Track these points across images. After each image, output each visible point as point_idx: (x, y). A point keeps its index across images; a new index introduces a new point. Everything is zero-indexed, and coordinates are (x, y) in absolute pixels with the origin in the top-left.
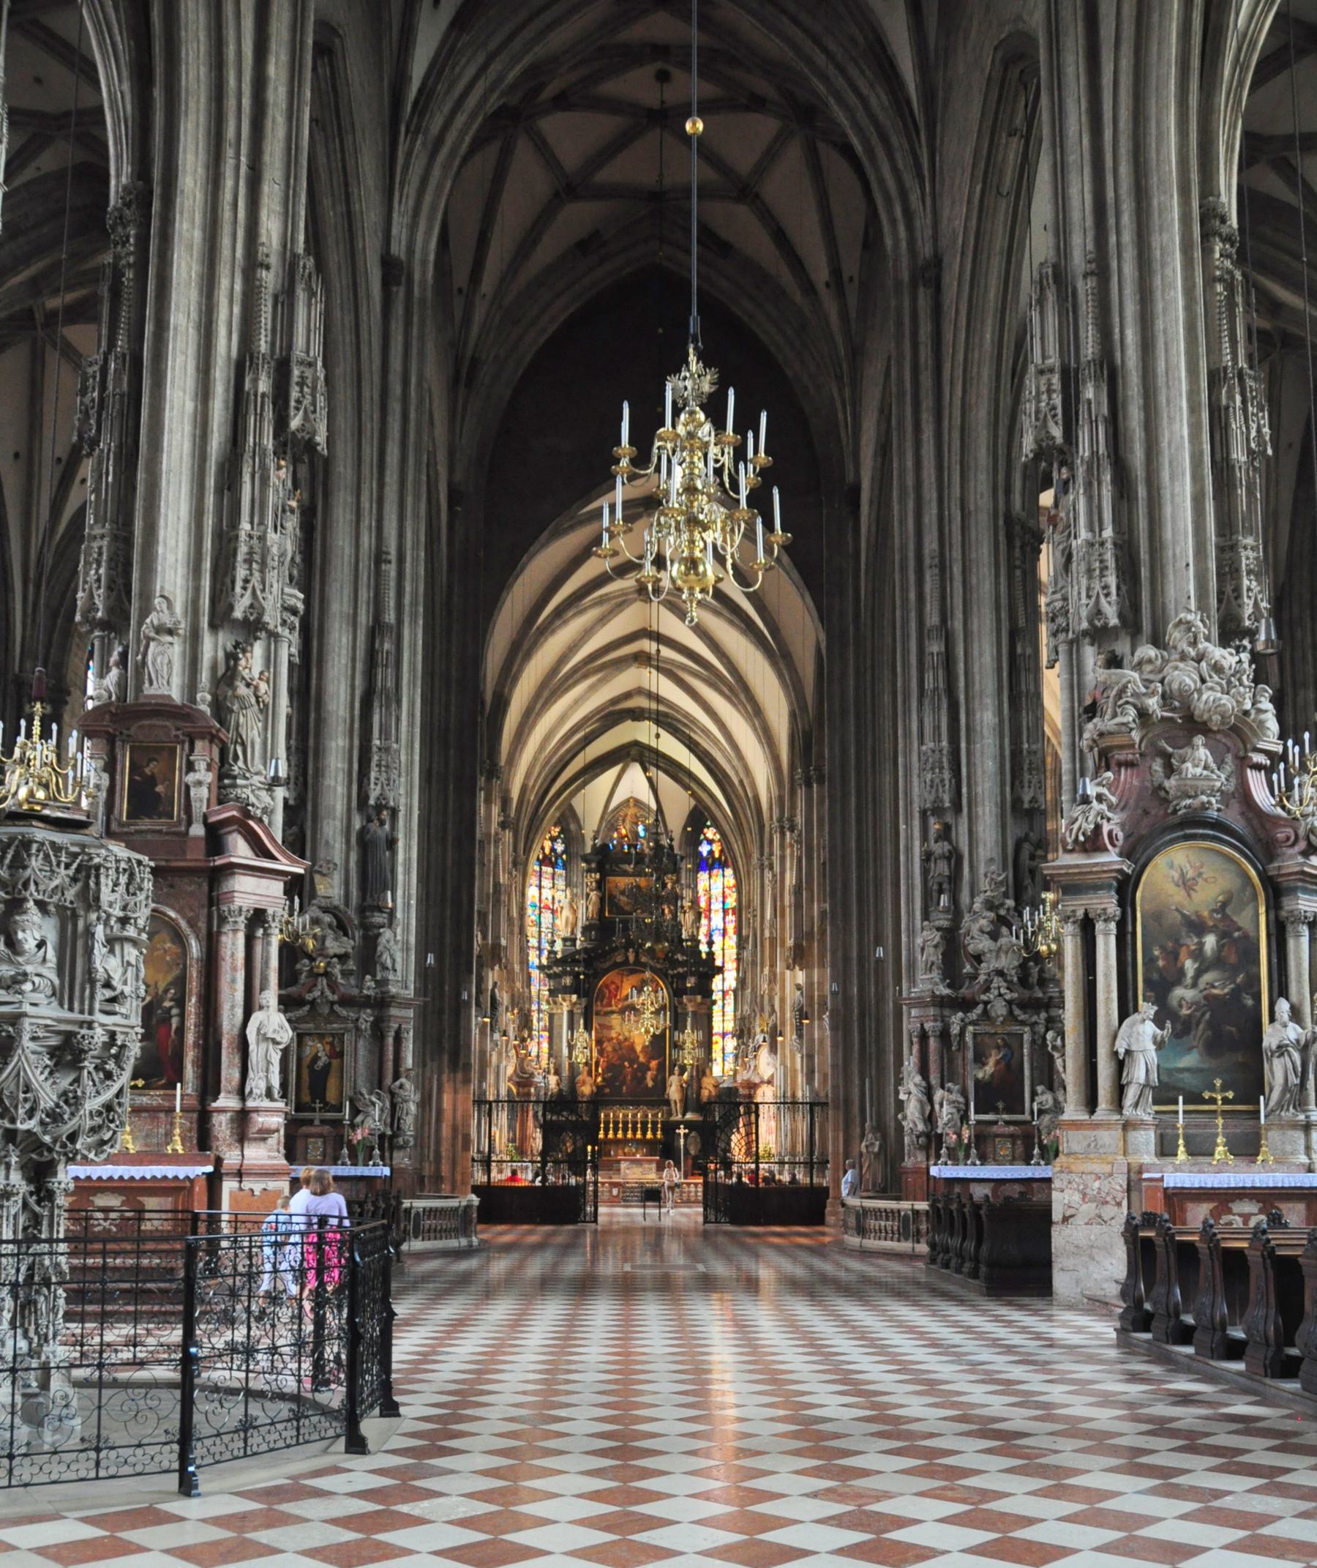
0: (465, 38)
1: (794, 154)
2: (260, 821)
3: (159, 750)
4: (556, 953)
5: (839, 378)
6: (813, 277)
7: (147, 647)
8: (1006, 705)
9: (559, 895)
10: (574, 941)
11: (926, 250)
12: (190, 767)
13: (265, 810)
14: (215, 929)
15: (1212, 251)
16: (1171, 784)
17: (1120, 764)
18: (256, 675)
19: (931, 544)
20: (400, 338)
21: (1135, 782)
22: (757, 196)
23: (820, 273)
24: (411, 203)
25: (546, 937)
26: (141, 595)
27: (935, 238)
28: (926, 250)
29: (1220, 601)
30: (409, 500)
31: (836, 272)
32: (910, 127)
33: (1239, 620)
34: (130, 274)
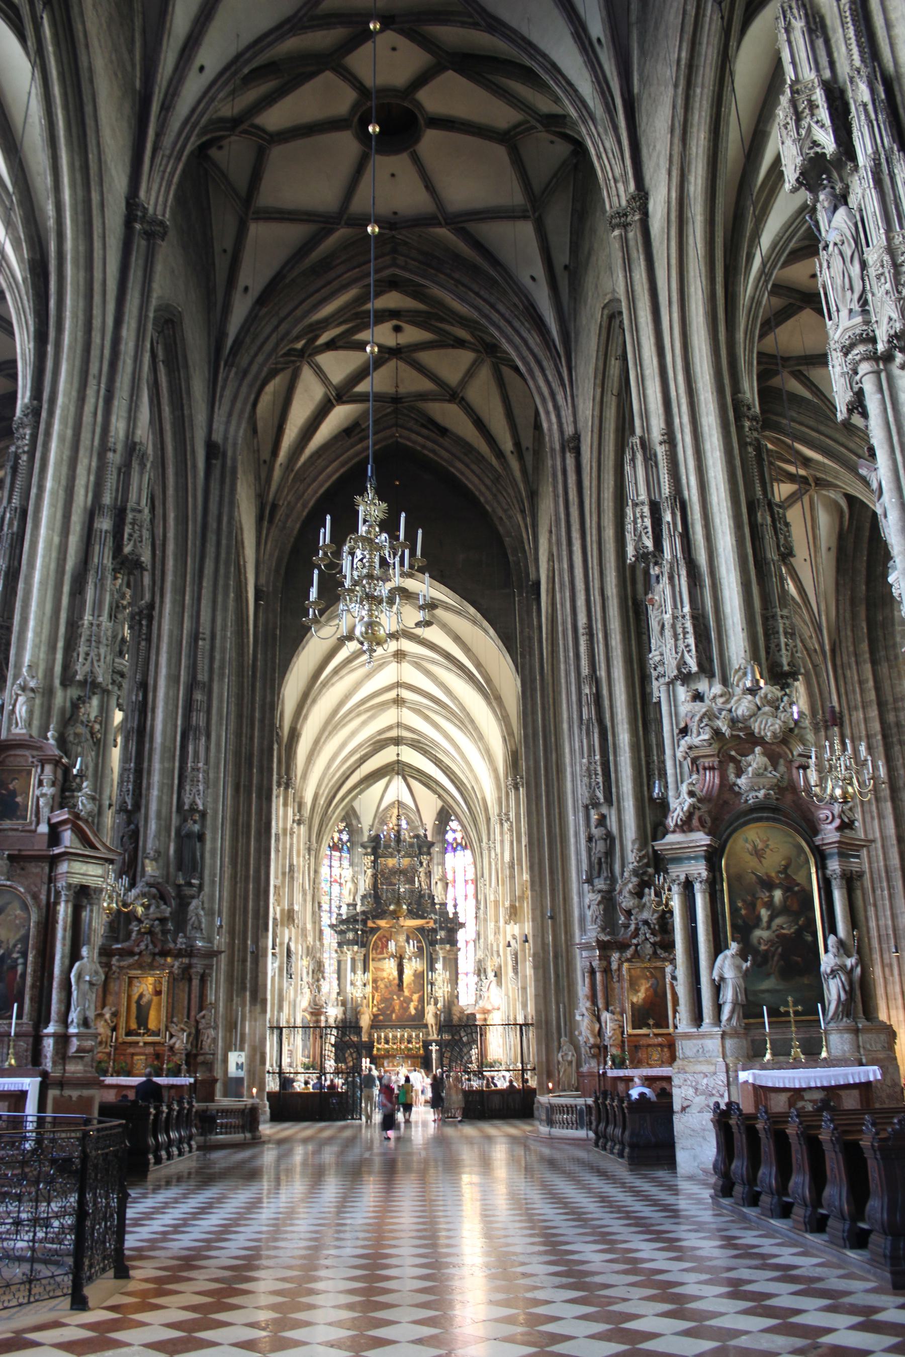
0: (264, 310)
1: (485, 373)
2: (86, 821)
3: (20, 771)
4: (341, 915)
5: (523, 511)
6: (503, 447)
7: (16, 700)
8: (641, 729)
9: (348, 873)
10: (355, 905)
11: (569, 430)
12: (40, 784)
13: (90, 814)
14: (52, 900)
15: (743, 427)
16: (742, 781)
17: (705, 769)
18: (92, 717)
19: (582, 620)
20: (217, 492)
21: (717, 781)
22: (463, 399)
23: (507, 445)
24: (225, 408)
25: (334, 904)
26: (15, 666)
27: (575, 422)
28: (569, 430)
29: (768, 653)
30: (220, 599)
31: (517, 444)
32: (555, 357)
33: (781, 666)
34: (25, 457)
